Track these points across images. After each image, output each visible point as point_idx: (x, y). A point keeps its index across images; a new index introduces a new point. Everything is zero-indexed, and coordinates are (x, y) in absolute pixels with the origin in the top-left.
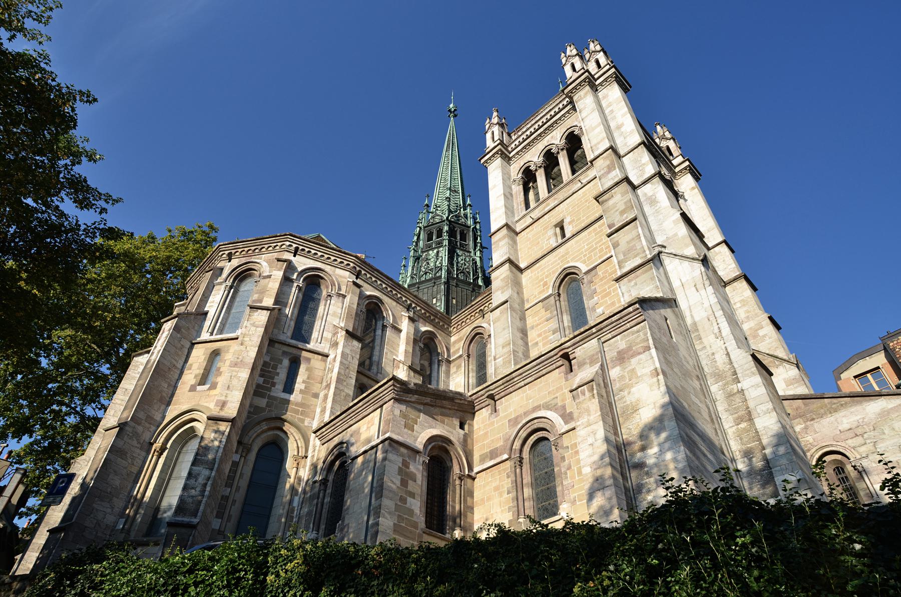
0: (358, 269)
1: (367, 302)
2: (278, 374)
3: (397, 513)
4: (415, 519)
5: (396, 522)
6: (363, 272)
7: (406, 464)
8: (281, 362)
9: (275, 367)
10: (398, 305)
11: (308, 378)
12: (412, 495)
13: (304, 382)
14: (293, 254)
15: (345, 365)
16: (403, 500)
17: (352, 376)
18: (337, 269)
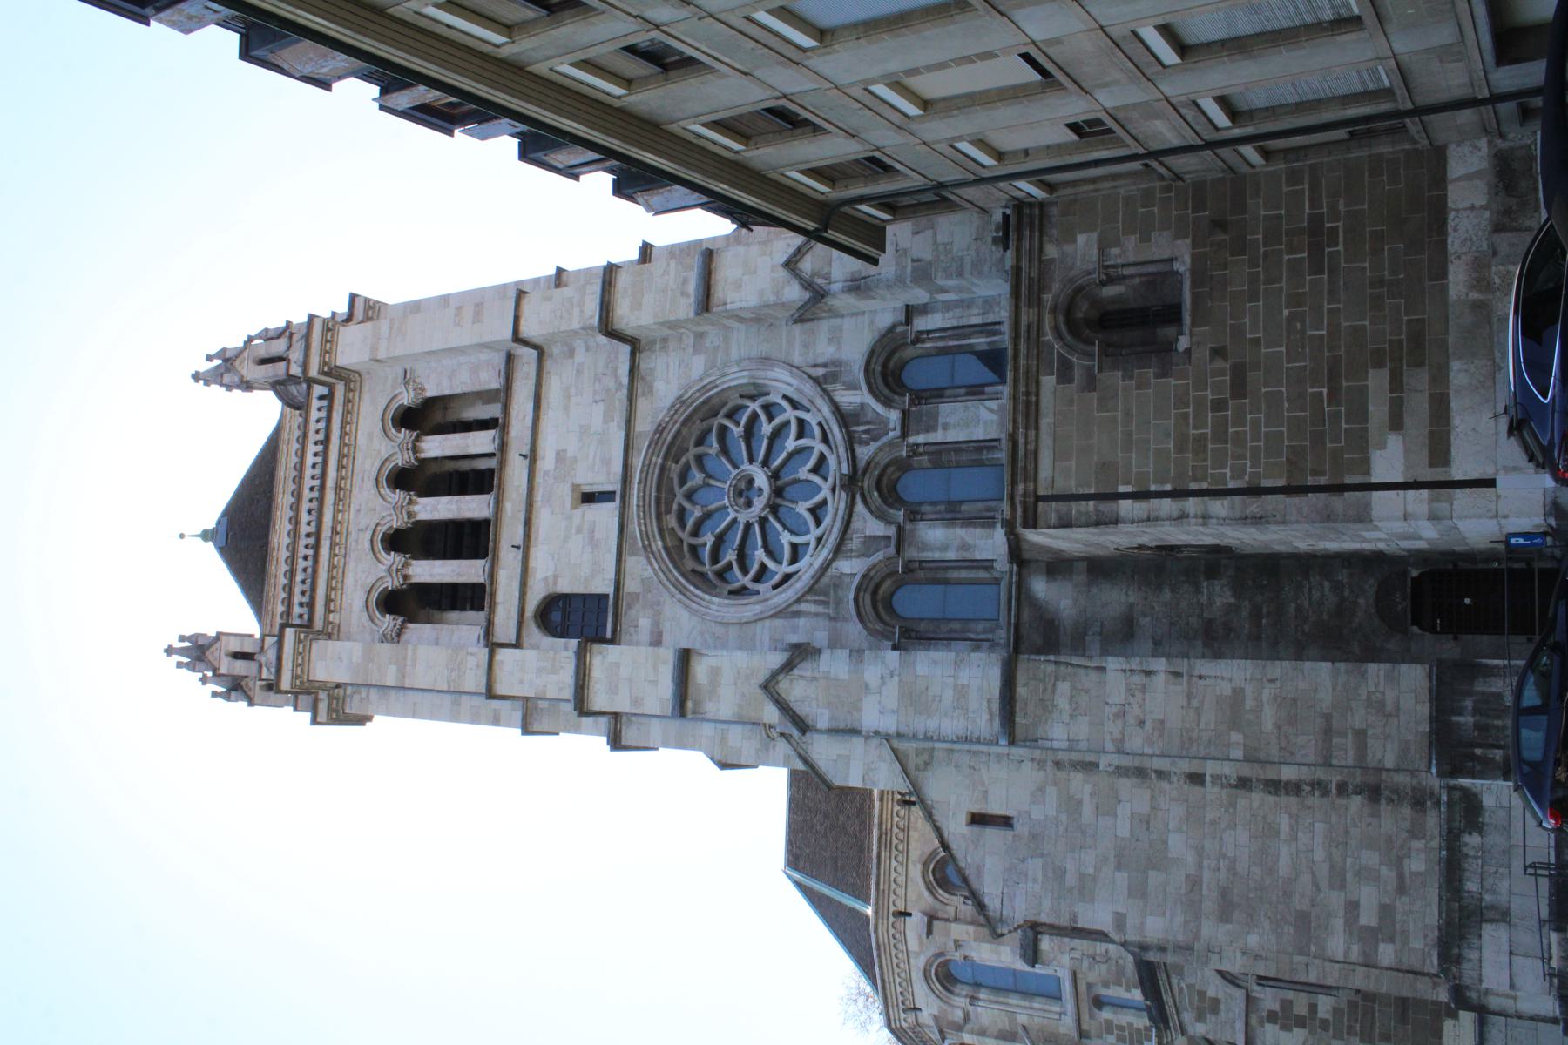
0: (892, 919)
1: (940, 891)
2: (1130, 1025)
3: (1345, 1037)
4: (1344, 1005)
5: (1358, 1039)
6: (892, 909)
7: (1272, 1017)
8: (1109, 1024)
9: (1121, 1028)
10: (911, 825)
11: (1121, 985)
12: (1313, 1008)
13: (1128, 990)
14: (918, 1013)
15: (1090, 963)
16: (1324, 1024)
17: (1103, 950)
18: (910, 948)
